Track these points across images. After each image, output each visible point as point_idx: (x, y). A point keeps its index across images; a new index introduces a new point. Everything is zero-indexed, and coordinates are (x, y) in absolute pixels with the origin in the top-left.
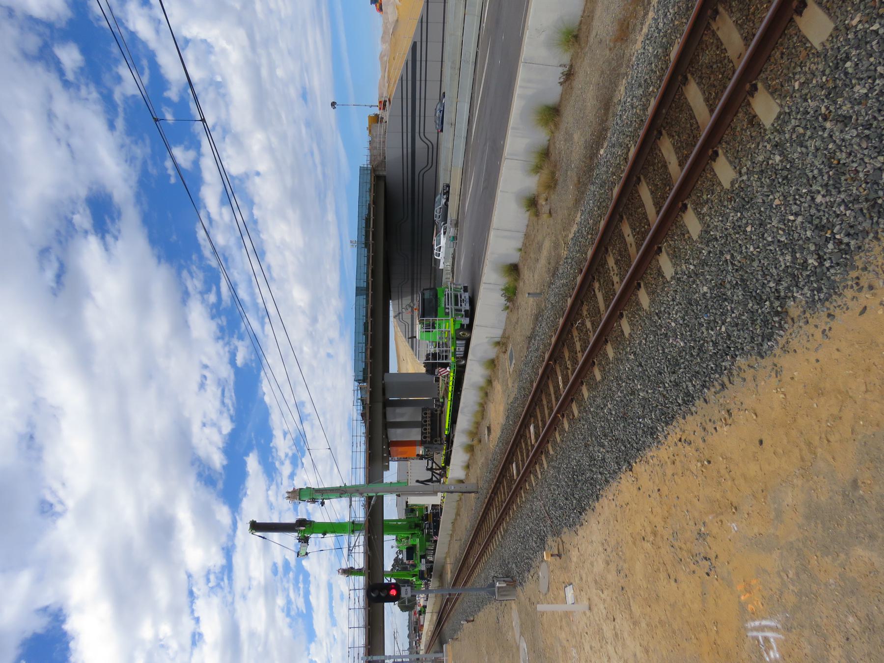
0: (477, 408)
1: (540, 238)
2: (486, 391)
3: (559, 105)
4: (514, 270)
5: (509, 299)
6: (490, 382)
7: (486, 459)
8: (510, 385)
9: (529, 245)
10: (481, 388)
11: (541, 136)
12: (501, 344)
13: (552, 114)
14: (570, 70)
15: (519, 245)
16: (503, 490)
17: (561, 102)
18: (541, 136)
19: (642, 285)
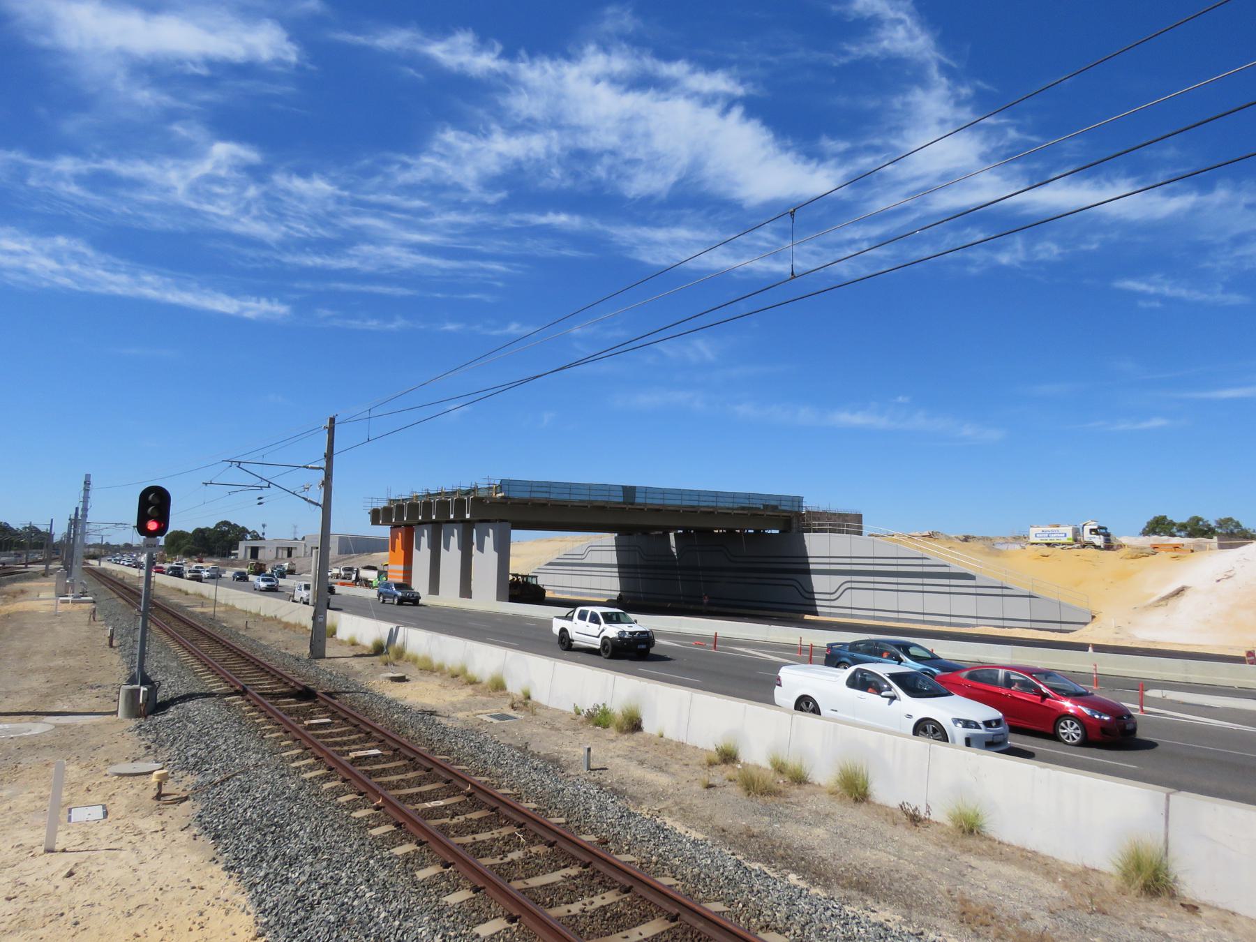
0: (436, 661)
1: (675, 767)
2: (460, 677)
3: (869, 802)
4: (634, 725)
5: (590, 716)
6: (472, 682)
7: (358, 673)
8: (461, 715)
9: (669, 753)
10: (464, 671)
11: (824, 774)
12: (525, 702)
13: (855, 789)
14: (920, 820)
15: (668, 734)
16: (300, 701)
17: (874, 803)
18: (824, 774)
19: (673, 924)
